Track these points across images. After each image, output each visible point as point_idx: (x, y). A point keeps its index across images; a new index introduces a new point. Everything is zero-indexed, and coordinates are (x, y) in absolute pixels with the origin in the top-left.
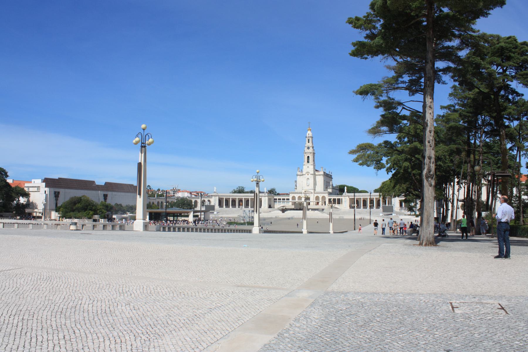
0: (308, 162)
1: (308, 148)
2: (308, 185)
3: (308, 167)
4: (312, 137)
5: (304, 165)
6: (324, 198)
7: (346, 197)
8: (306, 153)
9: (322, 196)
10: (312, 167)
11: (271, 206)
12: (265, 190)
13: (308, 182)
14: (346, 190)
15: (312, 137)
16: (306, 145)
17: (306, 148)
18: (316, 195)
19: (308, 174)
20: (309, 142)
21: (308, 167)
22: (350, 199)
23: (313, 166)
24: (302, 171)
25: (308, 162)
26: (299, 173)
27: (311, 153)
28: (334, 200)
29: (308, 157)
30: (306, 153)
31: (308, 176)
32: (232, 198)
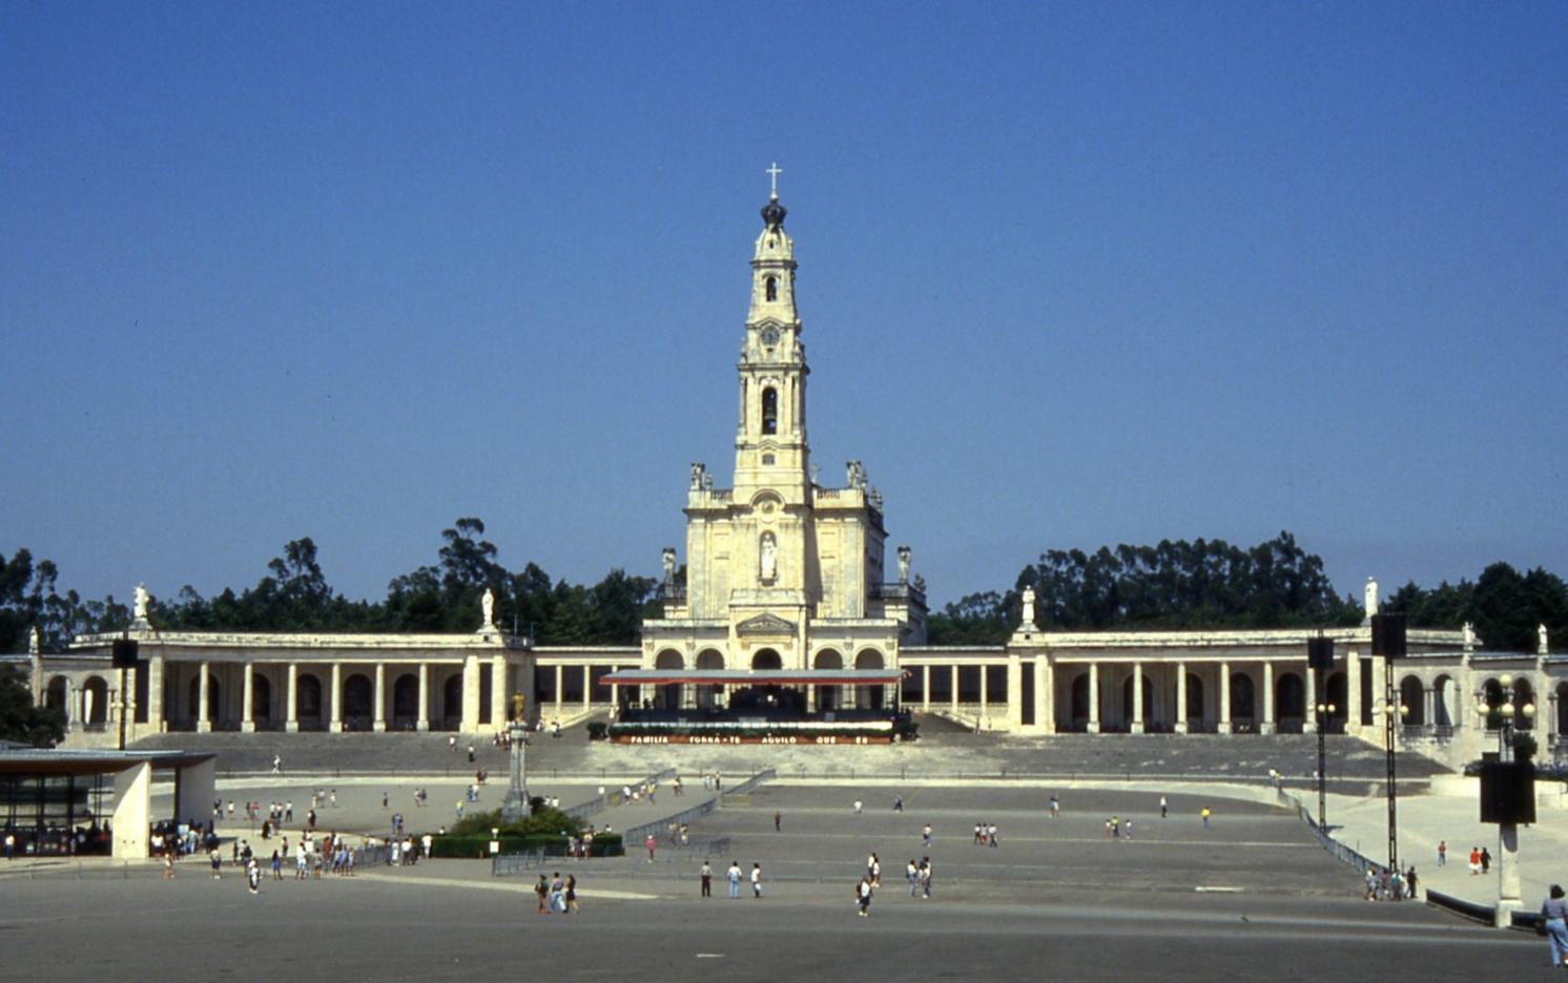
0: (768, 427)
3: (768, 460)
4: (790, 265)
5: (743, 447)
8: (752, 368)
15: (790, 265)
16: (755, 317)
17: (753, 336)
18: (819, 644)
19: (769, 509)
20: (771, 294)
22: (1059, 669)
23: (799, 452)
24: (723, 492)
25: (768, 427)
27: (786, 369)
30: (752, 368)
31: (768, 517)
32: (343, 667)
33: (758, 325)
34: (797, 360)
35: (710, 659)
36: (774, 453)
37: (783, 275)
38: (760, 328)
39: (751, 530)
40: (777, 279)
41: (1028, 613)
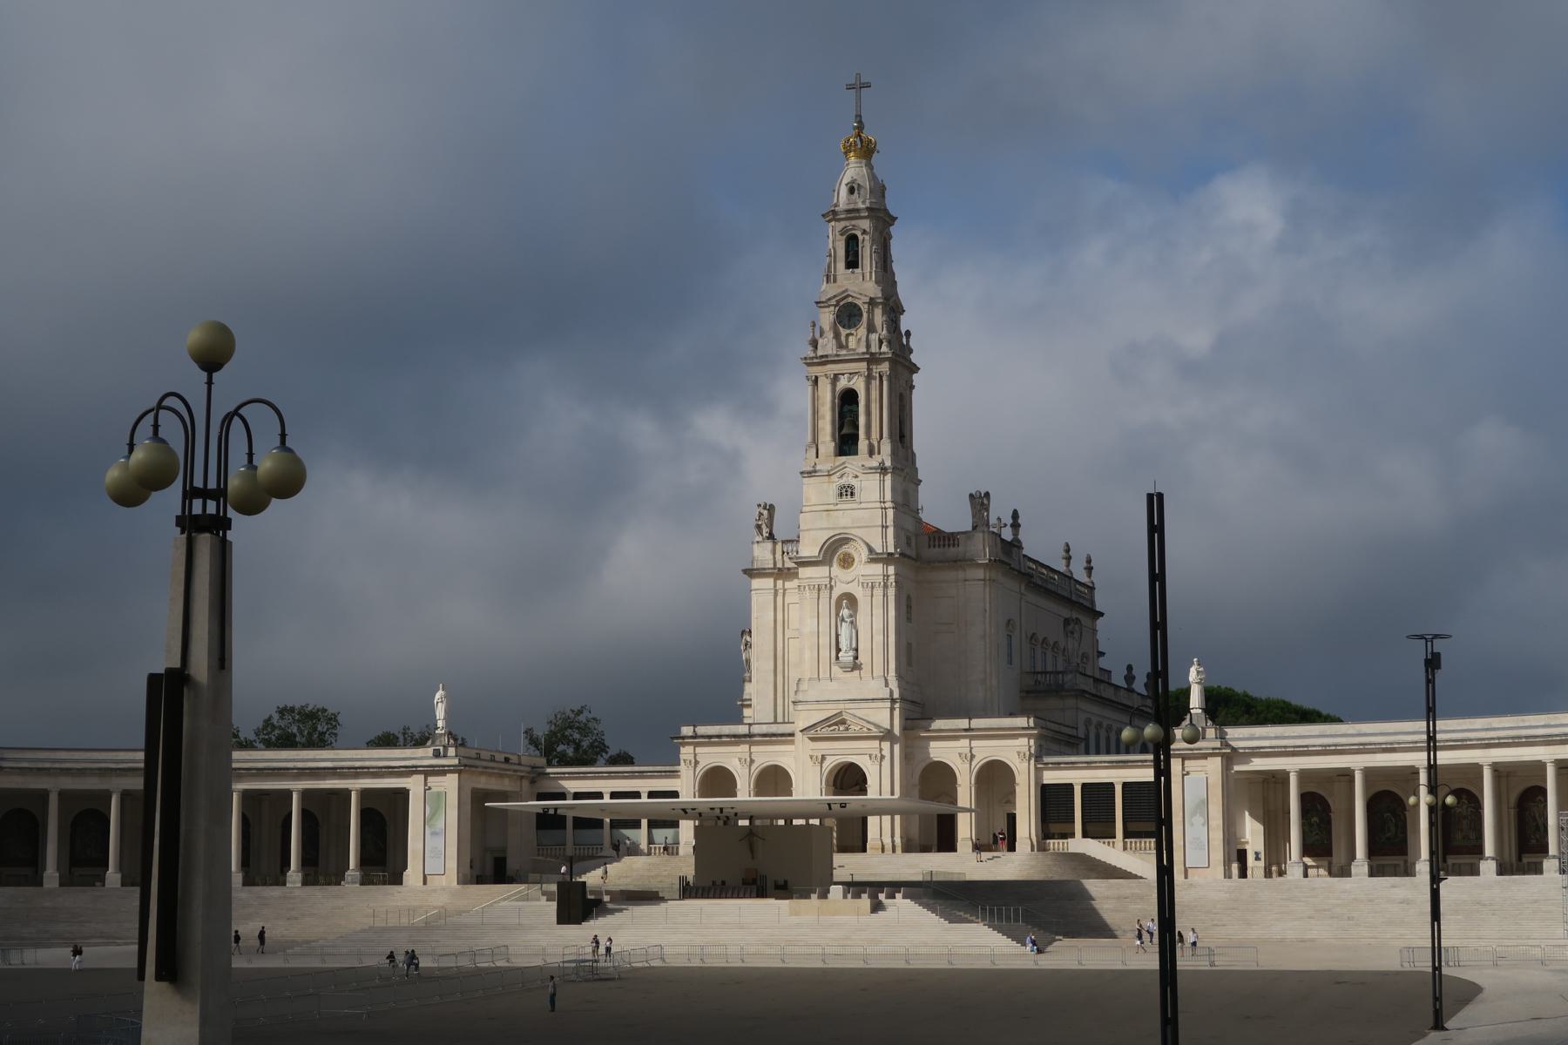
1: (848, 315)
2: (847, 657)
3: (847, 492)
5: (811, 473)
6: (995, 778)
7: (1205, 757)
9: (978, 762)
10: (874, 491)
11: (512, 865)
12: (440, 712)
13: (845, 630)
14: (1196, 700)
17: (827, 318)
19: (847, 562)
20: (852, 263)
21: (847, 492)
25: (846, 444)
26: (763, 554)
28: (1098, 795)
29: (849, 398)
31: (848, 574)
33: (833, 302)
34: (884, 348)
35: (774, 779)
36: (853, 482)
37: (866, 224)
38: (835, 306)
39: (825, 594)
40: (860, 238)
41: (1196, 700)
